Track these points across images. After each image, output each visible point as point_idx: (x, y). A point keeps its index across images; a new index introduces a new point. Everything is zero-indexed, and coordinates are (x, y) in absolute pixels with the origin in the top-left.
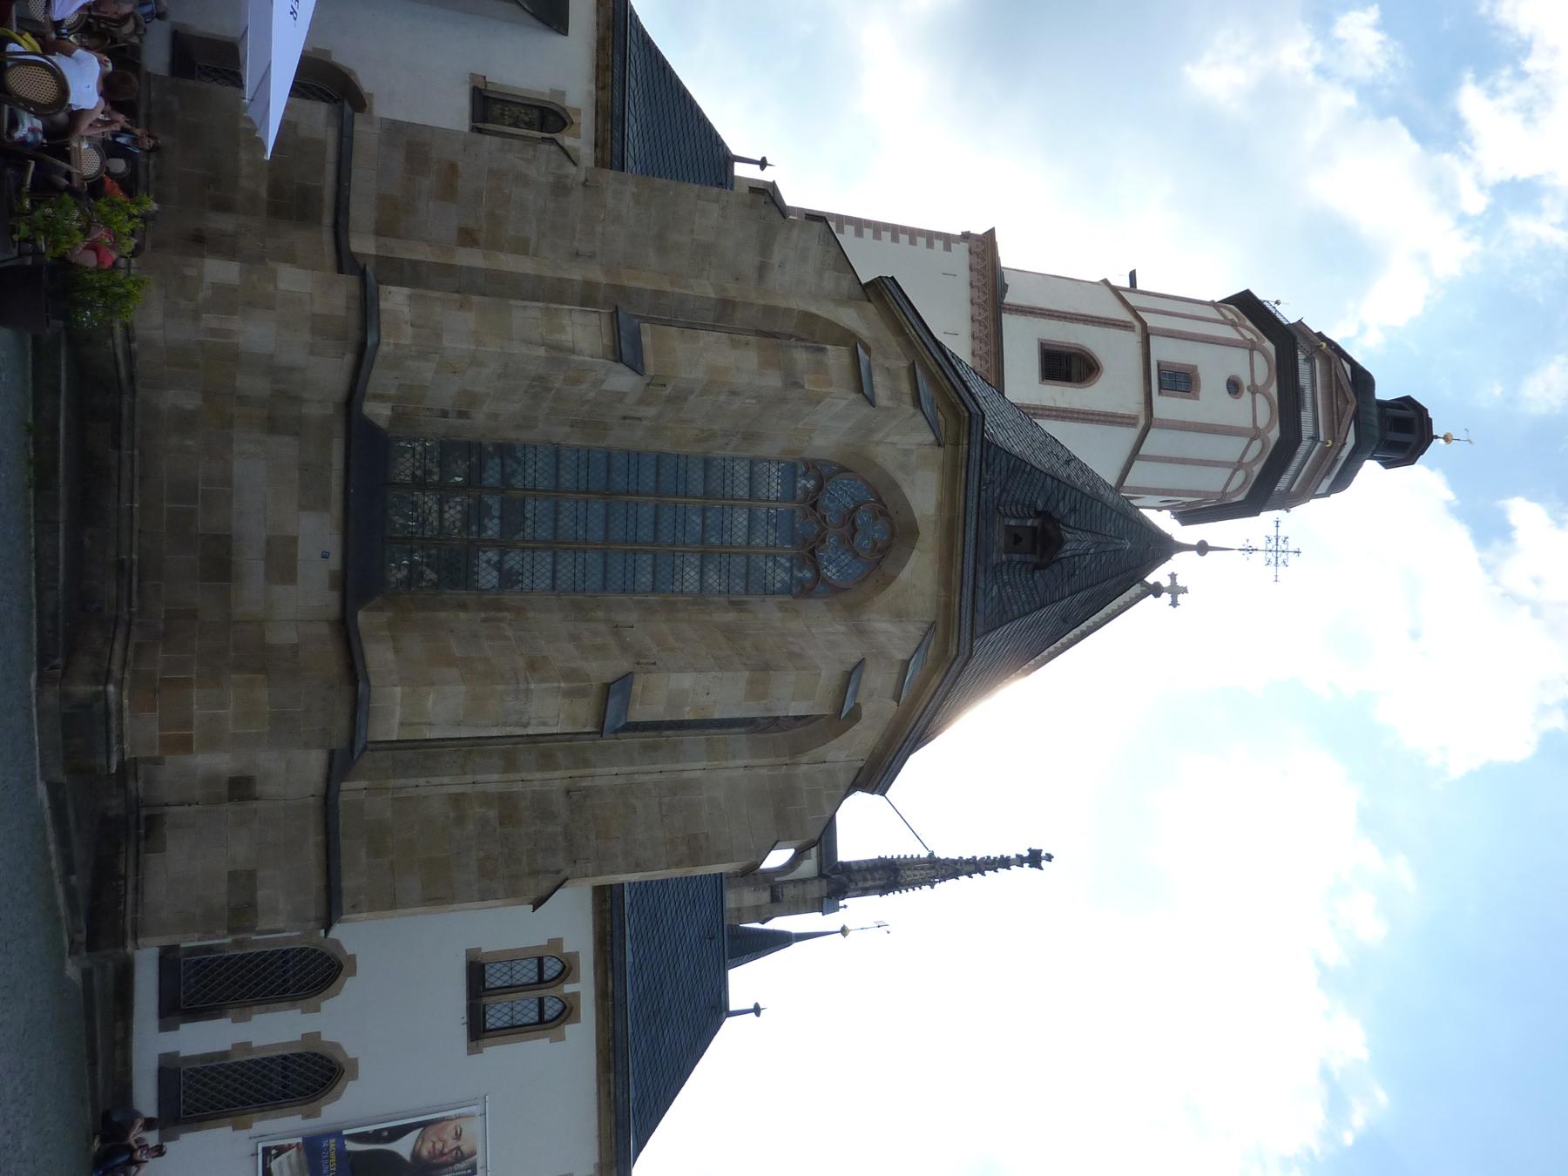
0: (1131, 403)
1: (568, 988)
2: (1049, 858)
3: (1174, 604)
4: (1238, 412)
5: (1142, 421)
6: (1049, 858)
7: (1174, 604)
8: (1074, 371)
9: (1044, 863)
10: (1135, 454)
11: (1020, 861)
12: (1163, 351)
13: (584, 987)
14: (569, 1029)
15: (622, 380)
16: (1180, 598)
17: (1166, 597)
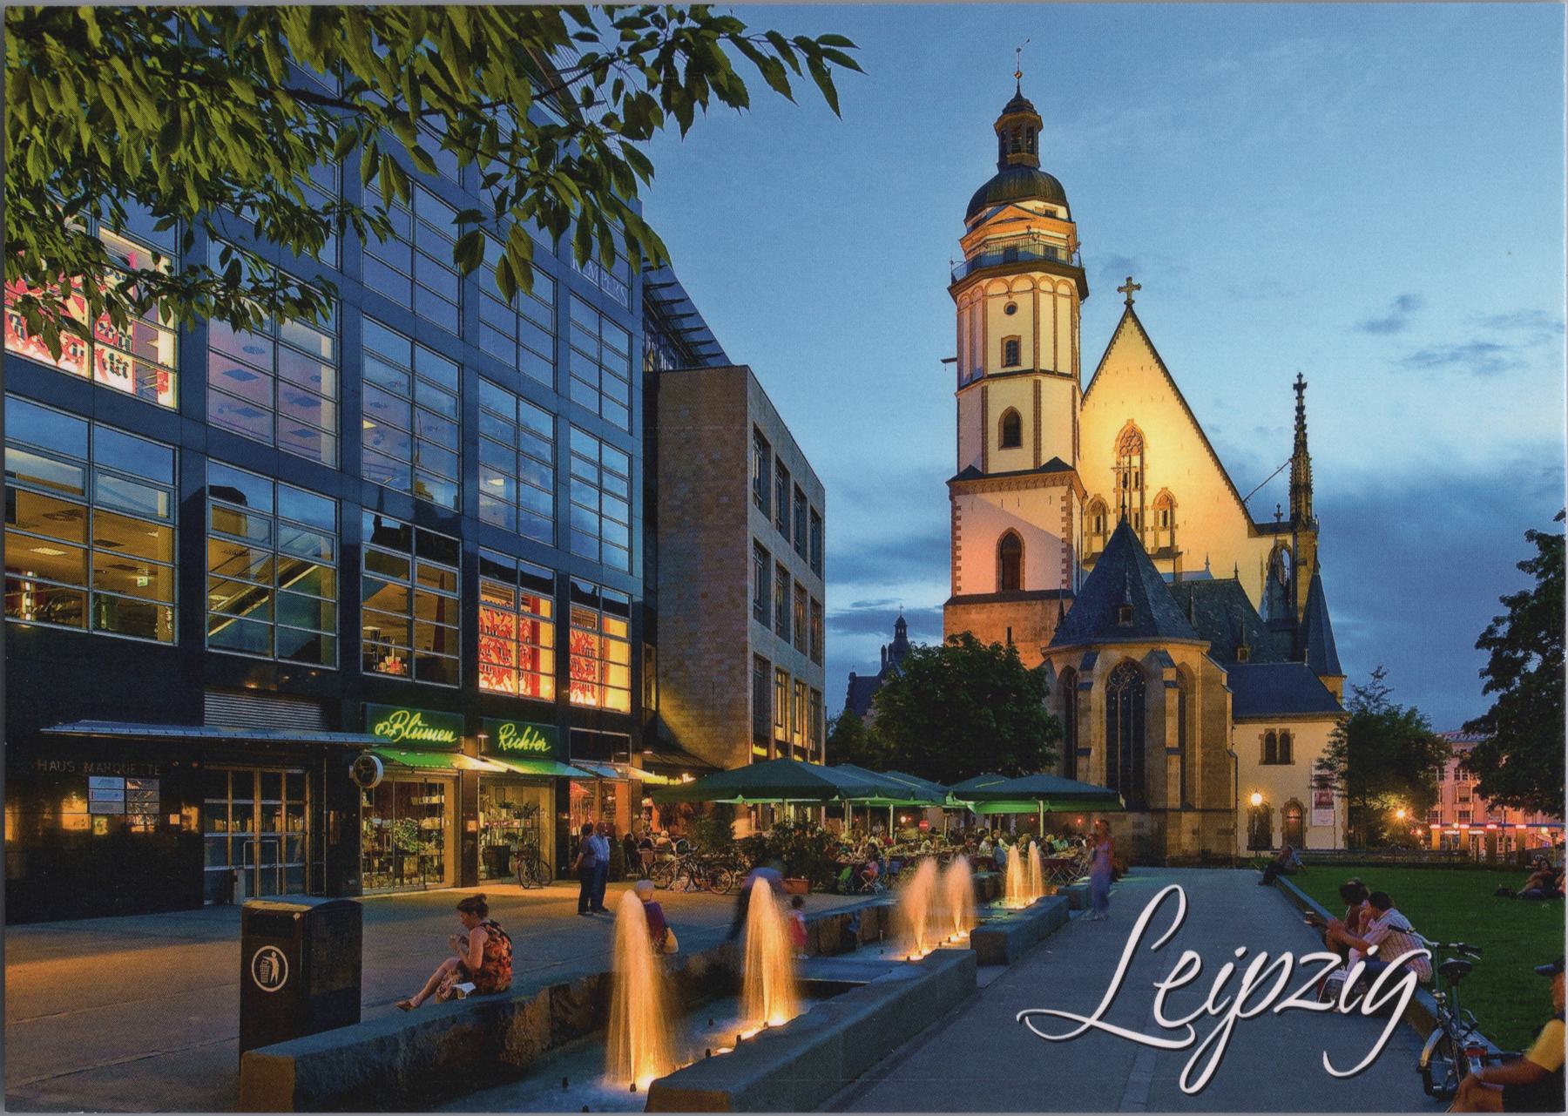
0: (1026, 384)
1: (1277, 732)
2: (1300, 376)
3: (1138, 287)
4: (1024, 303)
5: (1039, 378)
6: (1300, 376)
7: (1138, 287)
8: (1014, 422)
9: (1303, 382)
10: (1054, 373)
11: (1300, 398)
12: (995, 364)
13: (1278, 727)
14: (1291, 732)
15: (1093, 752)
16: (1135, 282)
17: (1135, 295)
